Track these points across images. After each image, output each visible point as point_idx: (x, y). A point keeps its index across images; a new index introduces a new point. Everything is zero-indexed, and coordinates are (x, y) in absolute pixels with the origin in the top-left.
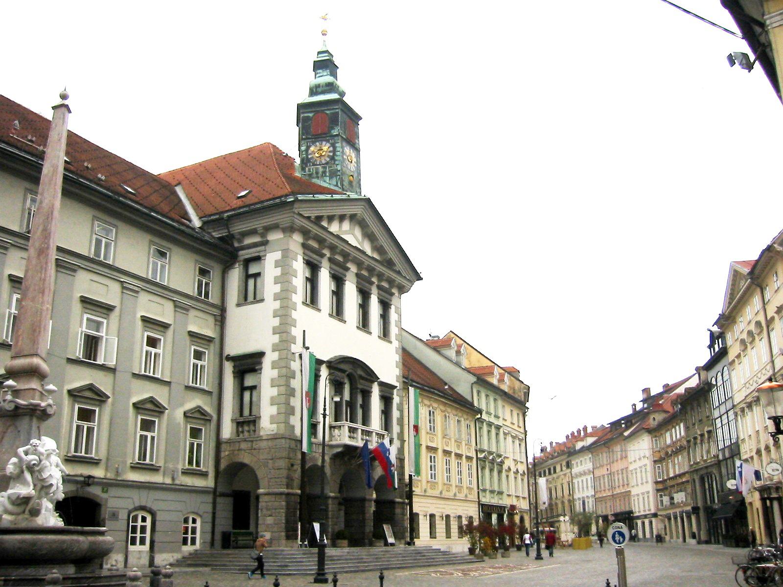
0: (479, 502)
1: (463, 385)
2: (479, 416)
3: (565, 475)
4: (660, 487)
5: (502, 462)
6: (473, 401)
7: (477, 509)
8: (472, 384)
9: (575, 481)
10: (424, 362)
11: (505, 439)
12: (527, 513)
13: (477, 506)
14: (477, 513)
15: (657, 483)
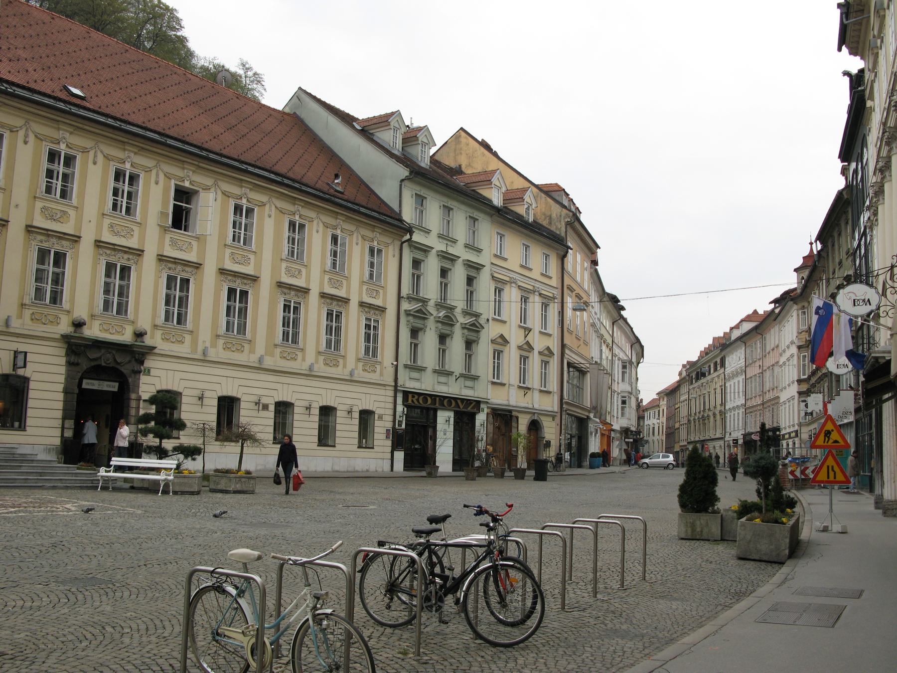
0: (396, 386)
1: (386, 180)
2: (408, 237)
3: (718, 376)
4: (804, 387)
5: (474, 328)
6: (400, 211)
7: (391, 400)
8: (402, 181)
9: (728, 385)
10: (336, 149)
11: (499, 291)
12: (554, 418)
13: (391, 393)
14: (391, 406)
15: (800, 381)
